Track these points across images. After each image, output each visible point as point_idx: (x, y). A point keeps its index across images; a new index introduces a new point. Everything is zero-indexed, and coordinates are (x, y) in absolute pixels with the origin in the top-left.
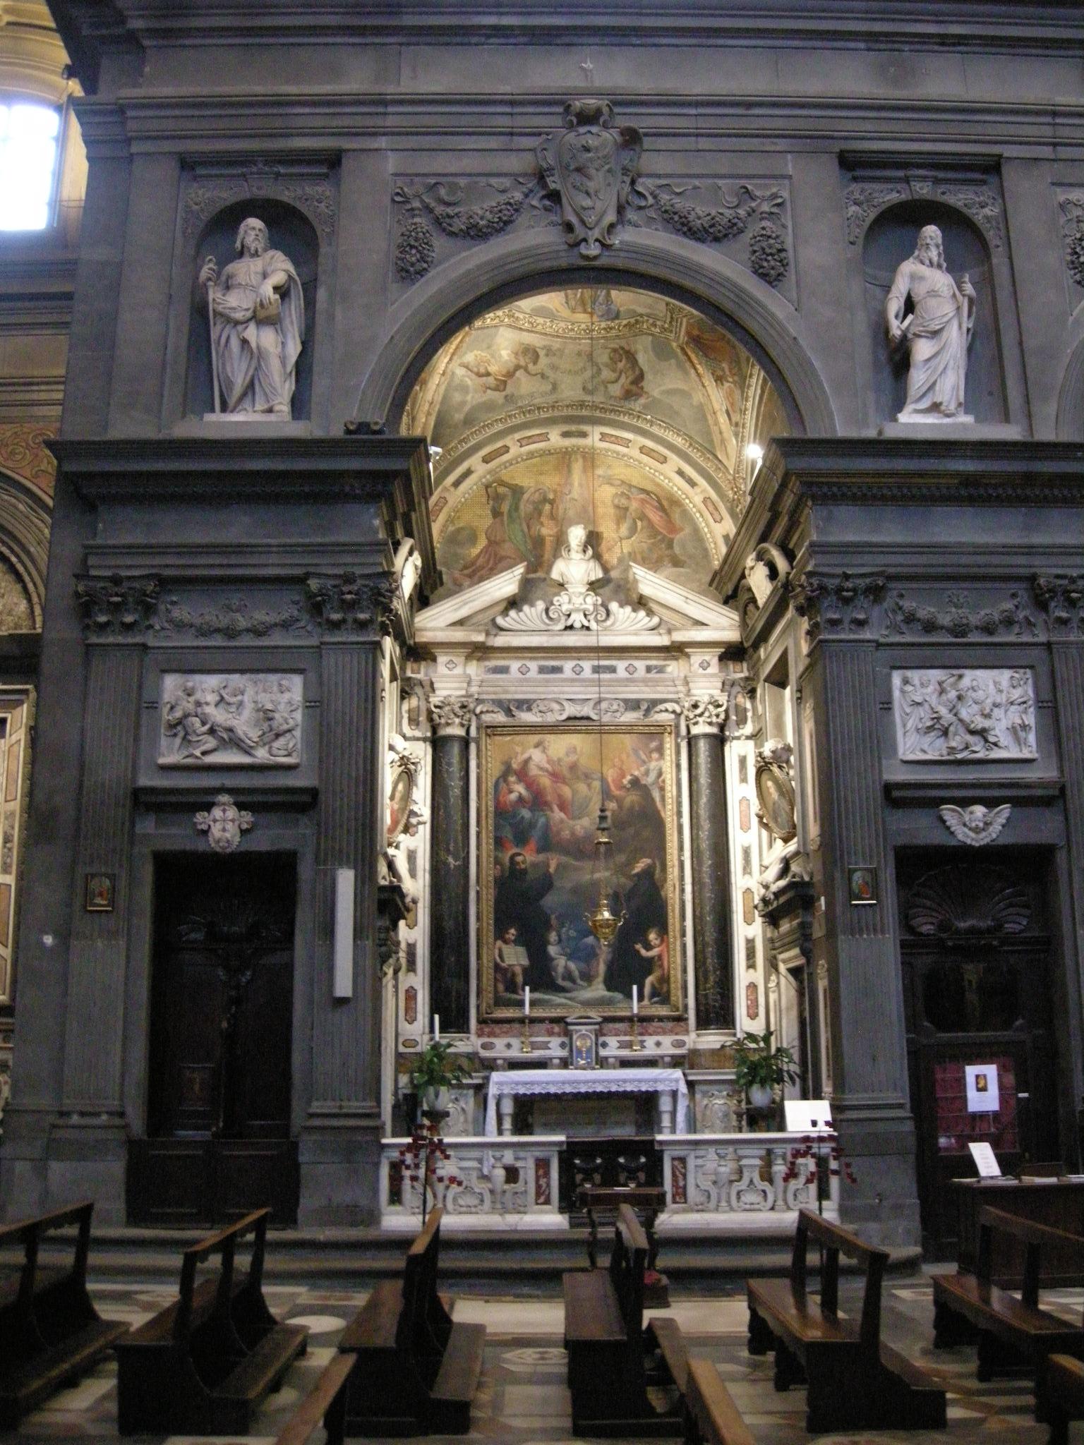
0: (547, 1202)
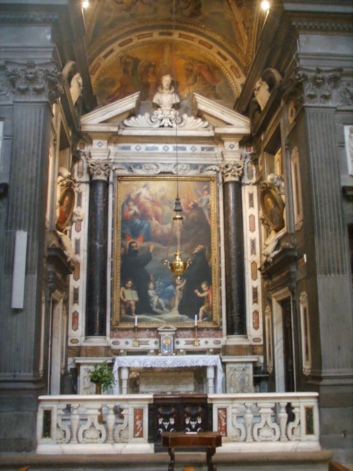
0: (141, 436)
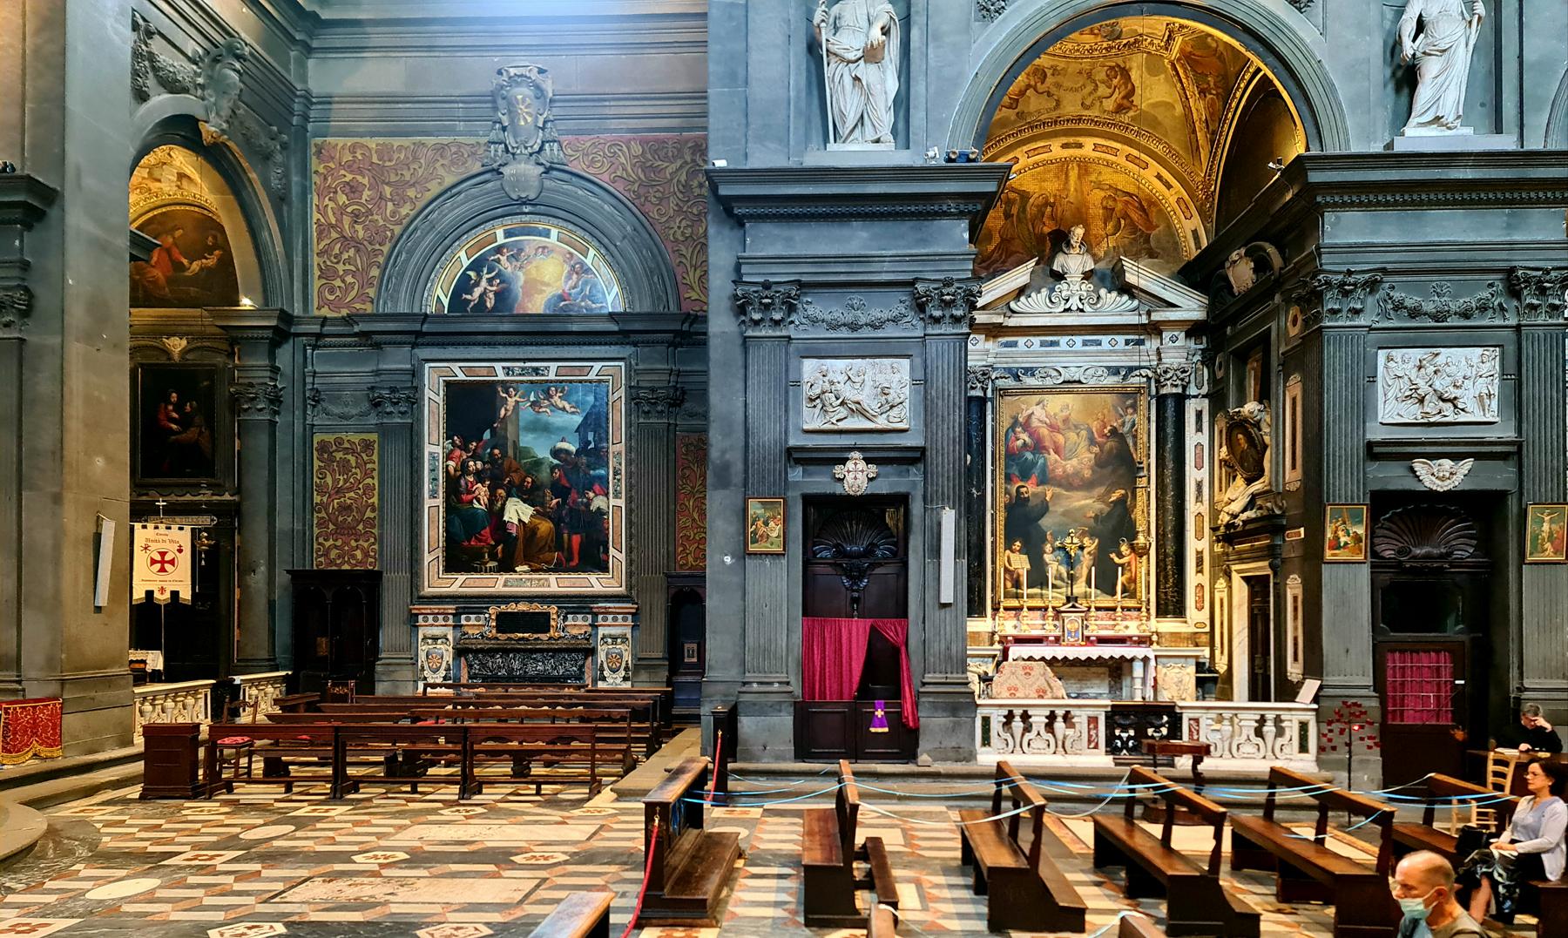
0: (1096, 747)
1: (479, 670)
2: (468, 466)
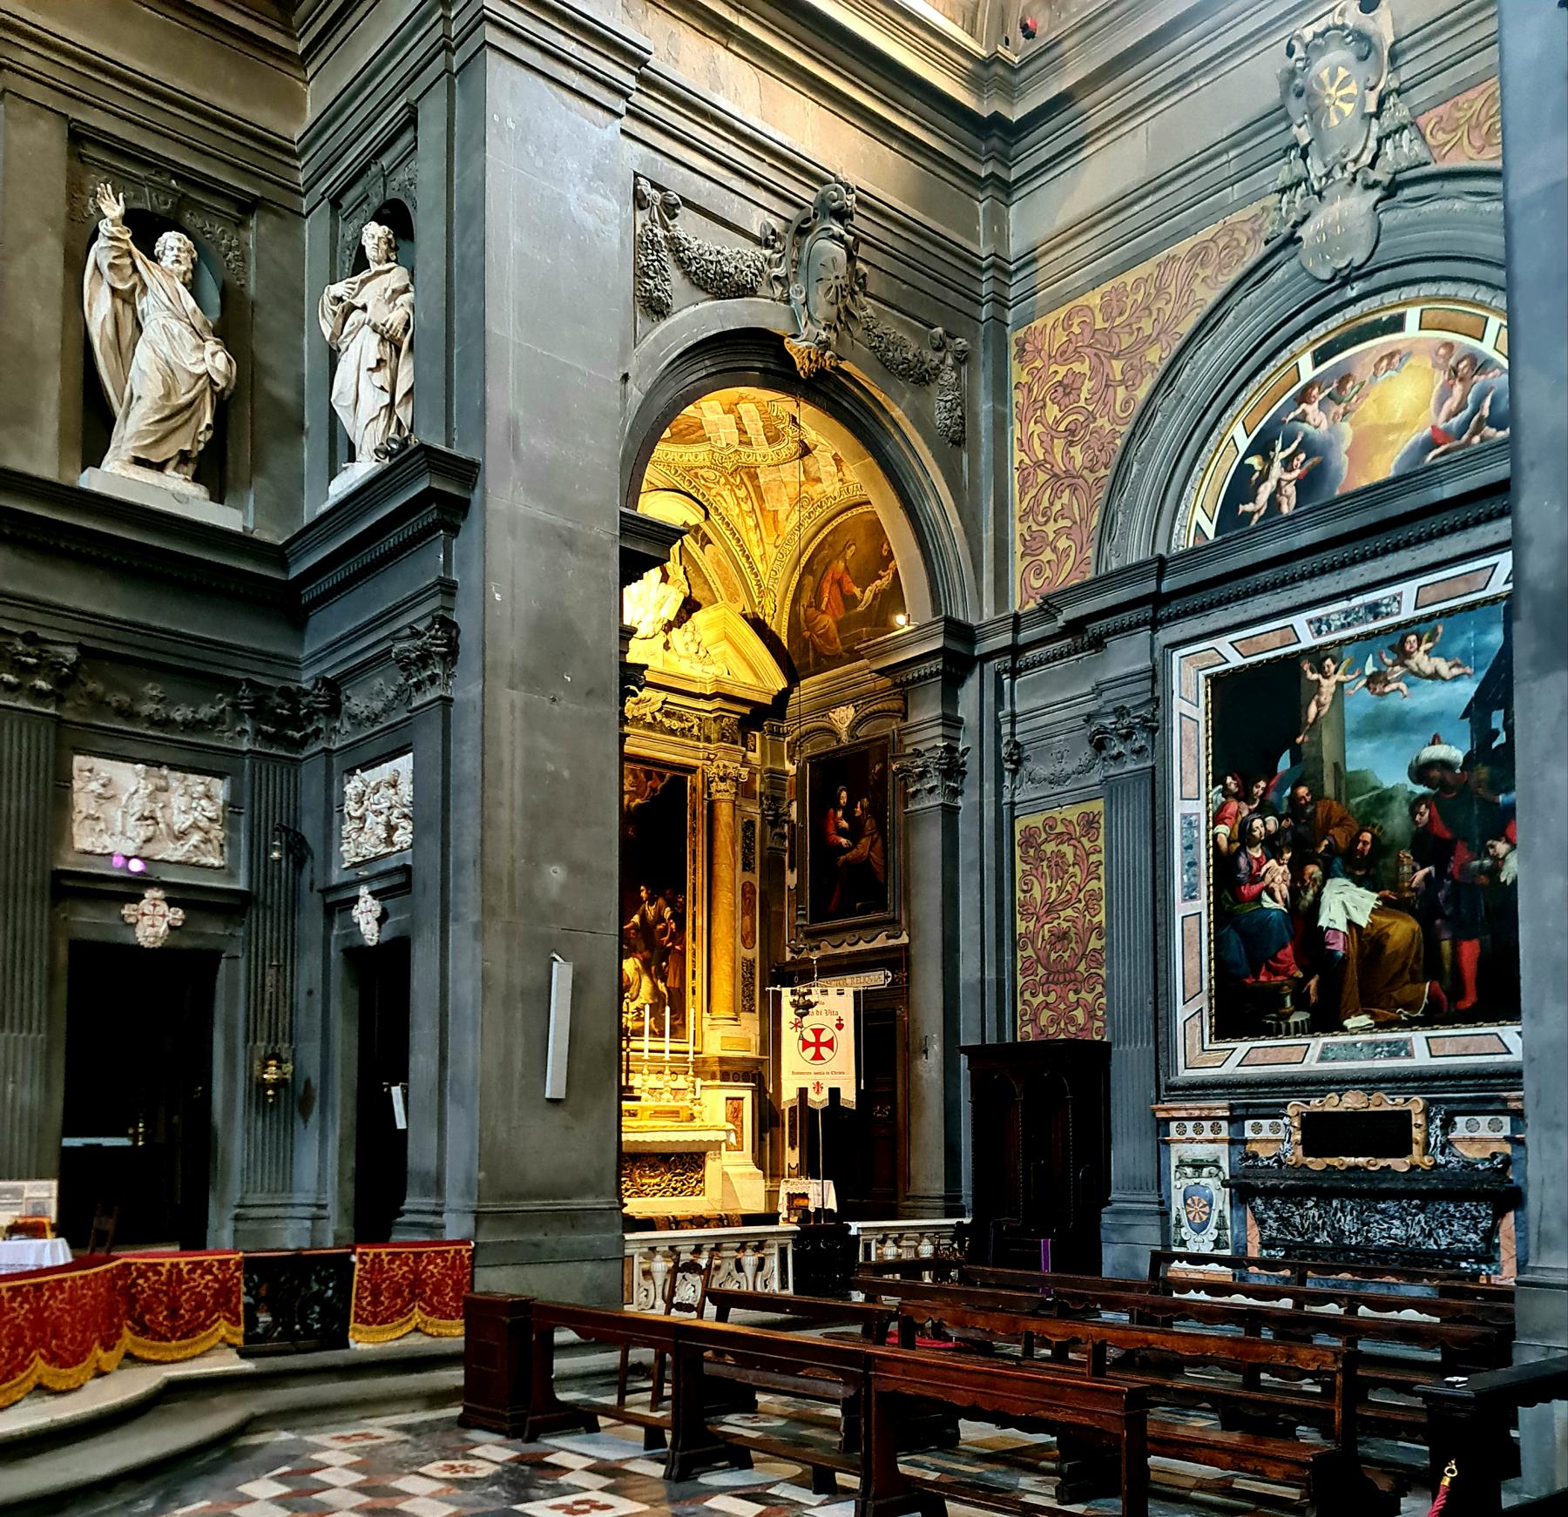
1: (1278, 1230)
2: (1251, 830)
